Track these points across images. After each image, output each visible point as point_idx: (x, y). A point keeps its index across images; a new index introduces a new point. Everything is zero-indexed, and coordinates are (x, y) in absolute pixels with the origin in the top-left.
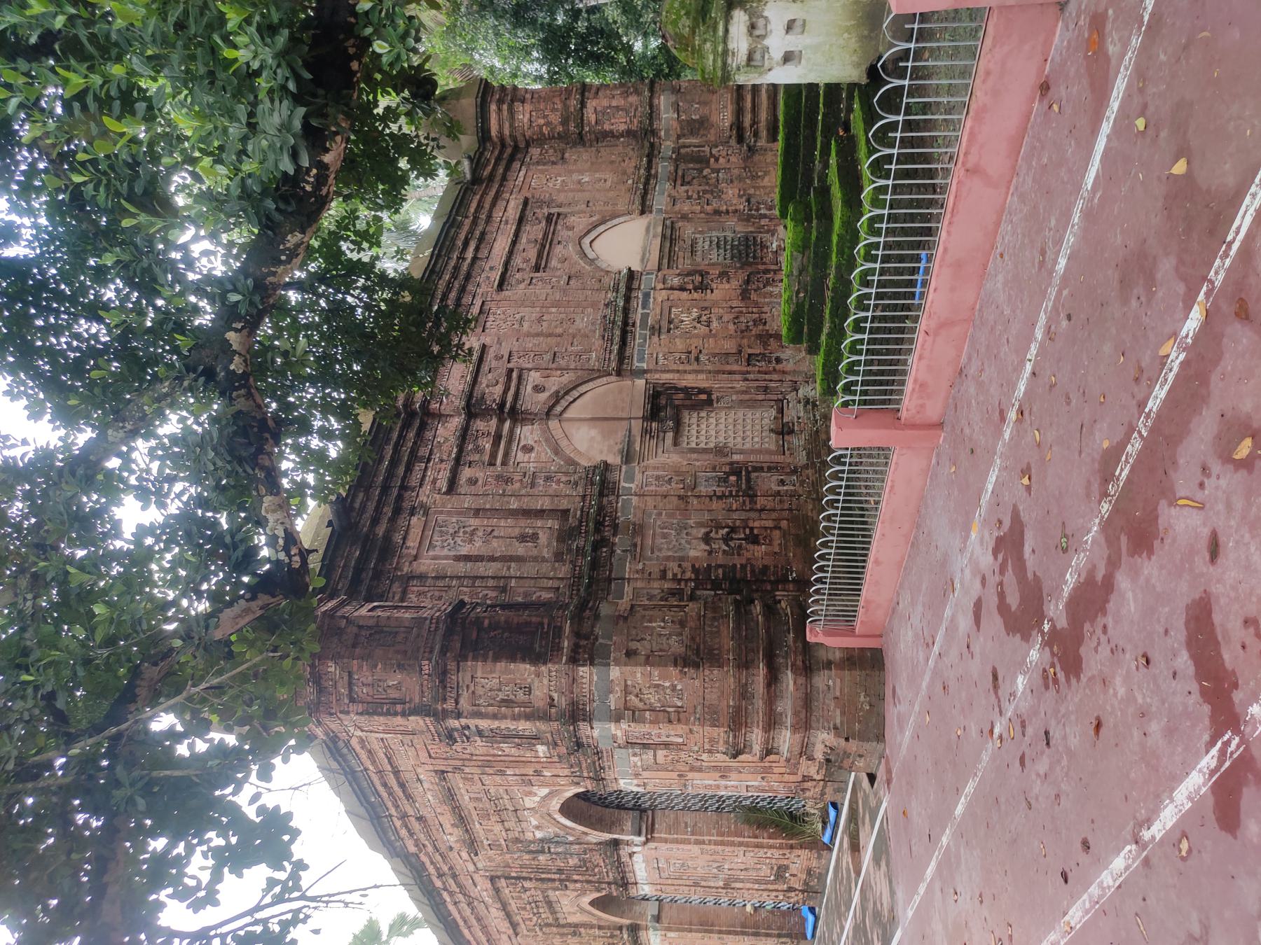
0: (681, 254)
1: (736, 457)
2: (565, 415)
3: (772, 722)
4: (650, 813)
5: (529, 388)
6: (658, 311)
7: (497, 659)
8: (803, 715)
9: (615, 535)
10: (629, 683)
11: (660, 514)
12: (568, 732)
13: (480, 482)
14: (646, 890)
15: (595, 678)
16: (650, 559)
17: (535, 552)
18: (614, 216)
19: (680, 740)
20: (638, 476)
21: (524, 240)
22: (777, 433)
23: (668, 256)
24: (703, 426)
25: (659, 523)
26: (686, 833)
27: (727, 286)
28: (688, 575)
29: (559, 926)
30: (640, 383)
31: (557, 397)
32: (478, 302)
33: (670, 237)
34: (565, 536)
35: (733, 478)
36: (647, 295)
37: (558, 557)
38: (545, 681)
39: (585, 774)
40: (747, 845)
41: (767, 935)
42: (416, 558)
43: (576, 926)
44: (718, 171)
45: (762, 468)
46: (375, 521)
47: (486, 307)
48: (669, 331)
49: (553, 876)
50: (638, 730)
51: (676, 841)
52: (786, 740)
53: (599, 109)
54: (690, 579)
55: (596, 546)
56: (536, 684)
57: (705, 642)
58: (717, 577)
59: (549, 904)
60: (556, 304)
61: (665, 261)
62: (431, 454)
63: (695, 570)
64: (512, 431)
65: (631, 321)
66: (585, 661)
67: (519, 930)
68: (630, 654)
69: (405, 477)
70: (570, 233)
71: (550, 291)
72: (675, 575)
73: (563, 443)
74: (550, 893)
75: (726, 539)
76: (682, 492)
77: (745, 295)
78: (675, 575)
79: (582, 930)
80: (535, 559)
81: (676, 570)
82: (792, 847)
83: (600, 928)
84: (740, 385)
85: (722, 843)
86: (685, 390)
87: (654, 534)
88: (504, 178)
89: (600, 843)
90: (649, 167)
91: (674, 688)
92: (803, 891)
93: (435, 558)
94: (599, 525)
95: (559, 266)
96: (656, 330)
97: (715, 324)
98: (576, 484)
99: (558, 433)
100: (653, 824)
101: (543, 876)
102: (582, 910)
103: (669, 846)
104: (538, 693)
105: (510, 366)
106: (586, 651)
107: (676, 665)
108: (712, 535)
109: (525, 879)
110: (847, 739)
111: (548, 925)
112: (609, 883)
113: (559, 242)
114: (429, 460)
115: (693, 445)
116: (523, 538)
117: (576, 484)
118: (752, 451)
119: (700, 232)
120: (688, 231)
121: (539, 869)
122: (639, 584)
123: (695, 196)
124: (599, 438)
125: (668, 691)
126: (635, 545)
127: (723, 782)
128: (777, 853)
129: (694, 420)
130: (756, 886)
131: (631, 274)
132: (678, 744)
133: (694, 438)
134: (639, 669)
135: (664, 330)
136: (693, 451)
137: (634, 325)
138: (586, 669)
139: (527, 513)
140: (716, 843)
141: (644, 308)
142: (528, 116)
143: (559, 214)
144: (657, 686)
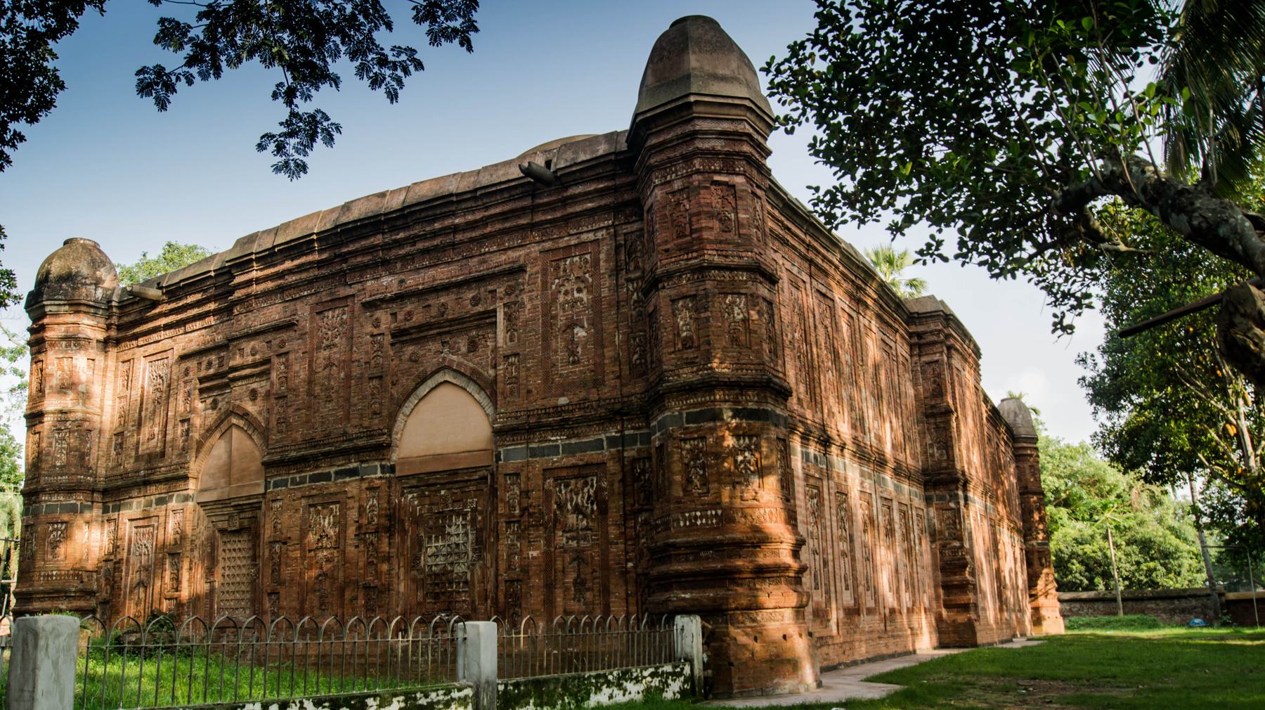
5: (254, 386)
24: (239, 555)
36: (353, 472)
48: (314, 506)
61: (414, 482)
88: (566, 219)
90: (587, 421)
105: (275, 360)
113: (443, 343)
119: (474, 520)
137: (317, 467)
141: (337, 473)
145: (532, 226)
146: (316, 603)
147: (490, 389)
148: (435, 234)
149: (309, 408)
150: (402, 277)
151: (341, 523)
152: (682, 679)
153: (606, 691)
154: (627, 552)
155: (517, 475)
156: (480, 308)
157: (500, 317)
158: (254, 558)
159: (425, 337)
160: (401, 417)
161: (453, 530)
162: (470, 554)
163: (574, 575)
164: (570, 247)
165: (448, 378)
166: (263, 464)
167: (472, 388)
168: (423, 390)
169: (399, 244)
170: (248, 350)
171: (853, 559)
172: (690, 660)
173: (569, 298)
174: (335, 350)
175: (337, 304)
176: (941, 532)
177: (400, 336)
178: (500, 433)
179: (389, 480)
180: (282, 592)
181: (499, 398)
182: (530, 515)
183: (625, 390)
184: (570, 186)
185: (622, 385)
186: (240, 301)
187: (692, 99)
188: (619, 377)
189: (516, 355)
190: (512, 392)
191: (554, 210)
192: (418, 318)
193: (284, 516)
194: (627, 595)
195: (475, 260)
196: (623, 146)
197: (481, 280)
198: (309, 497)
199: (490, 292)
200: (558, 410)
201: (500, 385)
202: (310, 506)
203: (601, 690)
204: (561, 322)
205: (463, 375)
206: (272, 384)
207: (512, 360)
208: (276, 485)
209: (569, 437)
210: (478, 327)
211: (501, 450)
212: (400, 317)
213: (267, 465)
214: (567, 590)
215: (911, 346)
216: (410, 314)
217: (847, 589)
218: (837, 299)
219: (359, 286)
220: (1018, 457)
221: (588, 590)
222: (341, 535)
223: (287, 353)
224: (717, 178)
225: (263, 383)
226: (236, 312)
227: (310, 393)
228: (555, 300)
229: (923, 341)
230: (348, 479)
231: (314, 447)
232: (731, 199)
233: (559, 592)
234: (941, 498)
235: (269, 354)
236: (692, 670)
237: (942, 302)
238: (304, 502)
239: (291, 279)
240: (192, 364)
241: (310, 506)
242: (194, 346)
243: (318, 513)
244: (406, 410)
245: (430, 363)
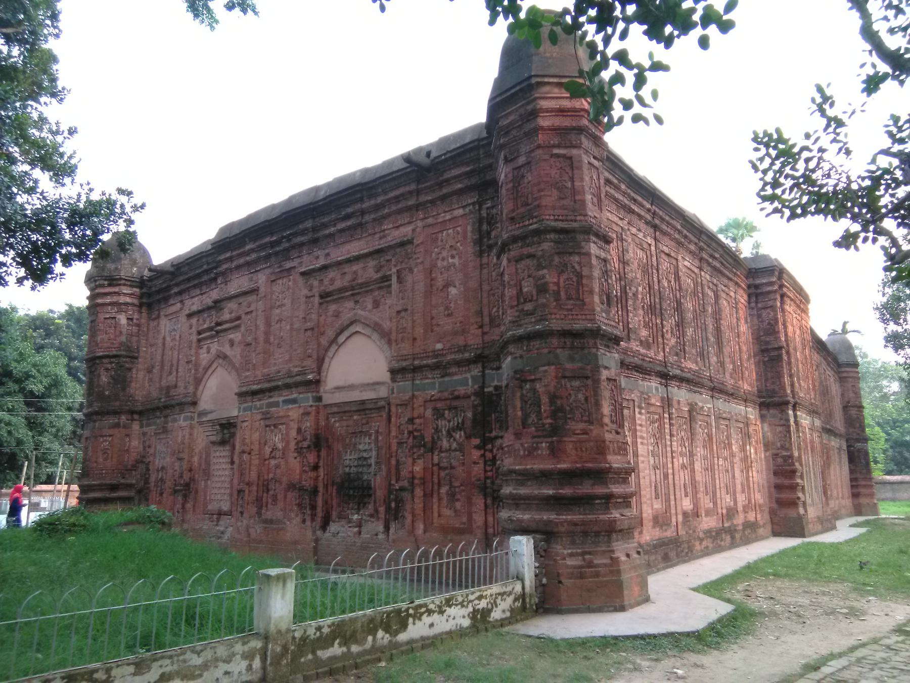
5: (232, 336)
6: (281, 414)
21: (355, 268)
34: (168, 388)
36: (294, 401)
42: (166, 316)
44: (461, 448)
46: (177, 285)
61: (335, 409)
65: (272, 394)
77: (291, 487)
90: (458, 363)
93: (165, 325)
96: (266, 417)
97: (273, 462)
105: (243, 316)
113: (357, 302)
120: (377, 424)
135: (268, 422)
136: (208, 455)
137: (271, 397)
141: (284, 402)
145: (417, 207)
146: (270, 500)
147: (386, 336)
148: (348, 217)
149: (265, 353)
150: (327, 251)
151: (285, 439)
152: (512, 597)
153: (426, 619)
154: (486, 471)
155: (406, 405)
156: (379, 275)
157: (394, 279)
158: (232, 463)
159: (342, 298)
160: (327, 360)
161: (361, 447)
162: (373, 466)
163: (447, 488)
164: (445, 221)
165: (358, 329)
166: (236, 394)
167: (375, 336)
168: (341, 339)
169: (325, 226)
170: (226, 311)
171: (693, 471)
172: (520, 578)
173: (445, 263)
174: (284, 308)
176: (773, 444)
177: (324, 296)
178: (393, 372)
179: (317, 407)
180: (247, 492)
181: (394, 344)
182: (415, 438)
183: (487, 338)
184: (445, 171)
185: (484, 334)
186: (223, 274)
187: (534, 80)
188: (481, 327)
189: (406, 310)
190: (402, 340)
191: (434, 191)
192: (338, 284)
193: (249, 433)
194: (486, 506)
195: (377, 236)
196: (485, 135)
197: (379, 252)
198: (265, 419)
199: (388, 261)
200: (436, 354)
201: (394, 334)
202: (267, 426)
203: (420, 619)
204: (440, 282)
205: (368, 325)
206: (243, 335)
207: (403, 314)
208: (245, 410)
209: (442, 377)
210: (380, 288)
211: (395, 385)
212: (326, 282)
213: (241, 395)
214: (440, 499)
215: (749, 296)
216: (332, 281)
217: (686, 496)
218: (680, 258)
219: (299, 260)
220: (842, 380)
221: (458, 500)
222: (285, 450)
223: (251, 312)
224: (556, 151)
225: (237, 334)
226: (219, 282)
227: (267, 341)
228: (434, 266)
229: (759, 291)
230: (290, 406)
231: (269, 381)
232: (568, 170)
233: (435, 500)
234: (774, 416)
235: (241, 312)
236: (523, 588)
237: (776, 259)
238: (262, 422)
239: (254, 256)
240: (194, 321)
241: (267, 426)
242: (195, 308)
243: (272, 431)
244: (330, 354)
245: (347, 316)
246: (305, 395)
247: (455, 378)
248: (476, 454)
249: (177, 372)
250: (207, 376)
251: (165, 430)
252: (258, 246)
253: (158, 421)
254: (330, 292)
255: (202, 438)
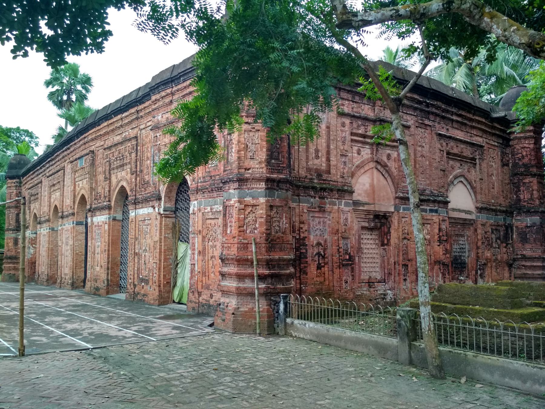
0: (457, 229)
1: (357, 258)
2: (375, 171)
3: (240, 277)
4: (174, 216)
5: (389, 152)
6: (429, 217)
7: (267, 141)
8: (244, 292)
9: (320, 198)
10: (257, 207)
11: (329, 220)
12: (233, 178)
13: (343, 128)
14: (132, 214)
15: (259, 191)
16: (308, 216)
17: (310, 158)
18: (475, 193)
19: (228, 232)
20: (347, 209)
21: (462, 146)
22: (369, 280)
23: (454, 222)
25: (326, 220)
26: (165, 234)
27: (441, 253)
28: (302, 235)
29: (110, 170)
30: (392, 209)
31: (385, 166)
32: (430, 123)
33: (465, 224)
35: (347, 257)
36: (436, 211)
37: (309, 170)
38: (257, 166)
39: (199, 184)
40: (160, 264)
41: (108, 274)
43: (110, 179)
45: (353, 272)
47: (428, 128)
49: (138, 167)
50: (234, 212)
51: (161, 229)
52: (231, 284)
53: (532, 184)
54: (300, 236)
55: (314, 188)
56: (256, 162)
57: (277, 244)
58: (301, 249)
59: (122, 166)
60: (430, 165)
61: (453, 221)
62: (356, 102)
63: (304, 238)
64: (367, 143)
66: (268, 185)
67: (107, 150)
68: (271, 207)
69: (344, 89)
70: (466, 170)
71: (437, 160)
72: (302, 228)
73: (362, 171)
74: (129, 166)
75: (319, 254)
76: (340, 231)
78: (302, 228)
79: (108, 182)
80: (307, 158)
81: (304, 229)
82: (159, 286)
83: (109, 191)
84: (392, 260)
85: (160, 252)
86: (389, 232)
87: (320, 217)
89: (159, 191)
91: (255, 229)
92: (134, 292)
94: (323, 189)
95: (450, 165)
98: (343, 177)
99: (366, 168)
100: (168, 217)
101: (138, 163)
102: (119, 182)
103: (158, 225)
104: (252, 162)
106: (272, 185)
107: (267, 229)
108: (320, 246)
109: (137, 153)
110: (233, 314)
111: (110, 165)
112: (135, 196)
113: (461, 165)
114: (353, 102)
115: (362, 237)
116: (317, 151)
117: (343, 177)
118: (360, 267)
119: (467, 239)
120: (469, 232)
121: (142, 161)
122: (297, 210)
123: (486, 236)
124: (365, 188)
125: (254, 226)
126: (315, 208)
127: (196, 252)
128: (156, 279)
129: (374, 237)
130: (136, 269)
131: (446, 203)
132: (226, 231)
133: (365, 237)
134: (264, 212)
138: (264, 186)
139: (328, 153)
140: (160, 249)
142: (527, 146)
143: (475, 164)
144: (256, 221)
161: (461, 242)
175: (423, 126)
178: (480, 210)
230: (434, 214)
246: (443, 209)
247: (499, 217)
248: (505, 250)
249: (328, 160)
250: (359, 173)
251: (322, 210)
252: (411, 98)
253: (312, 200)
254: (451, 153)
255: (354, 222)
